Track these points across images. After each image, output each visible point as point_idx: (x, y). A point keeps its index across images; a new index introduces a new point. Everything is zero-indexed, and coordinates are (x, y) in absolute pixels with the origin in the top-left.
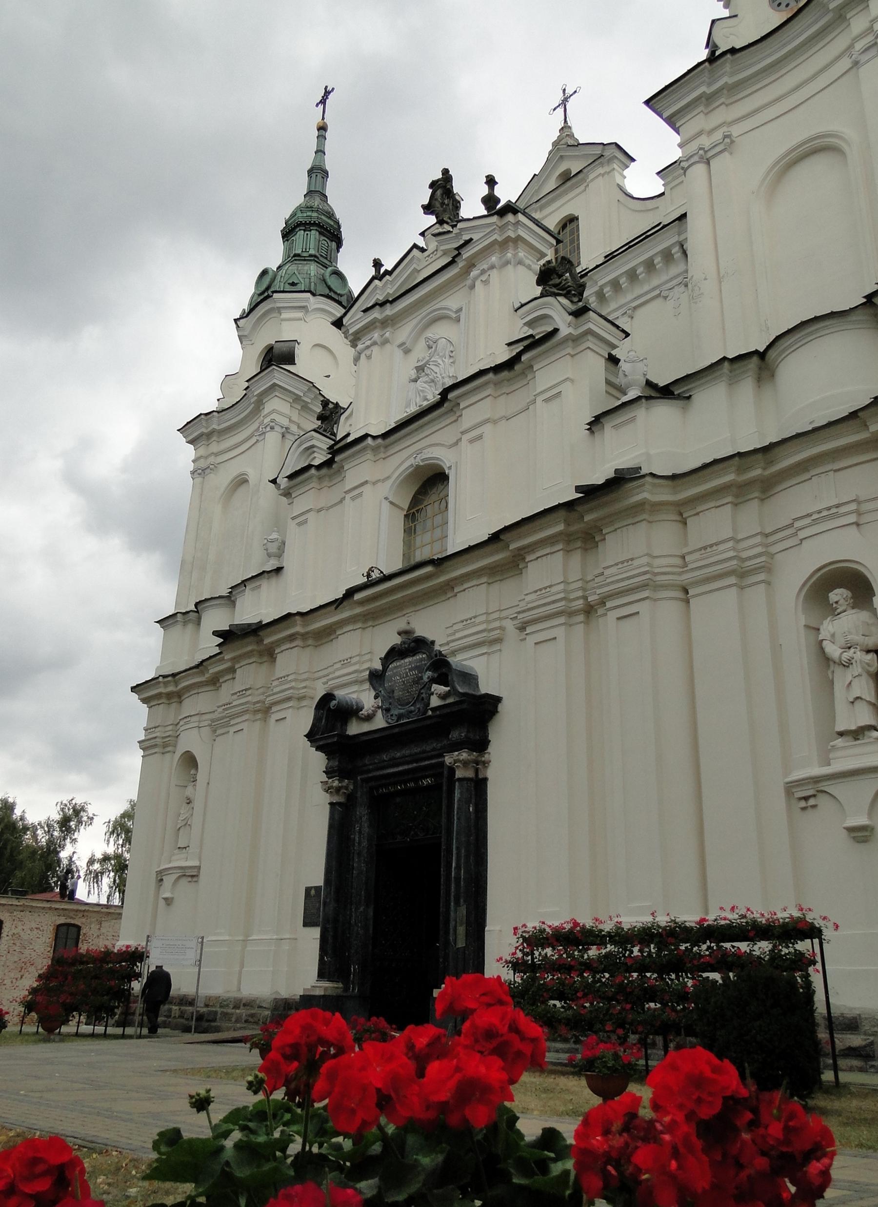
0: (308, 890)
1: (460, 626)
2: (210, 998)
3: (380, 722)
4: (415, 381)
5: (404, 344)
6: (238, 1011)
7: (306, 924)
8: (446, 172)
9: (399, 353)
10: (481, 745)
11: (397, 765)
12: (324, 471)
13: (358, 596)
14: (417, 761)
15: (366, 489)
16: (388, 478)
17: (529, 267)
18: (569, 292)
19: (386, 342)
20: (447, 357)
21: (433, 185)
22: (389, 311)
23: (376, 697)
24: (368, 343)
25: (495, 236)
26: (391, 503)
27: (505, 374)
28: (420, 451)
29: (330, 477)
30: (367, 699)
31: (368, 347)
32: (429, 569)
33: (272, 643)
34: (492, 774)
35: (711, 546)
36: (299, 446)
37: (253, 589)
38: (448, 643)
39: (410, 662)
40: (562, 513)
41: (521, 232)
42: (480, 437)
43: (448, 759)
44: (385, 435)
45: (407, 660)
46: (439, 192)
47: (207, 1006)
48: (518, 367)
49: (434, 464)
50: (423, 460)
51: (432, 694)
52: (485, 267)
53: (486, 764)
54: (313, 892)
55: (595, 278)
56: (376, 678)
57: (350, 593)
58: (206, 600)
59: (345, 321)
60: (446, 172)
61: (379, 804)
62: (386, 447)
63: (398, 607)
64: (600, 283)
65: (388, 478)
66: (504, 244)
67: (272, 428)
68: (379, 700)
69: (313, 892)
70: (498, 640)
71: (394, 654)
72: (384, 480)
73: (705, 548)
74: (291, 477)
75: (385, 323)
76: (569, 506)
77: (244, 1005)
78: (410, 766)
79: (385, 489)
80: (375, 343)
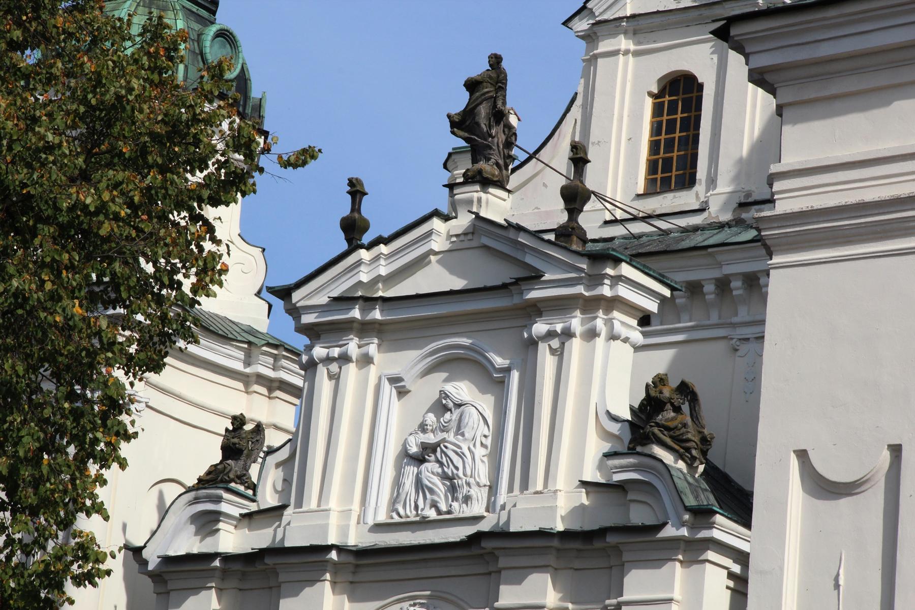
8: (496, 61)
17: (626, 340)
18: (688, 450)
20: (478, 444)
21: (472, 85)
25: (580, 289)
27: (577, 545)
41: (623, 291)
46: (483, 111)
48: (598, 544)
52: (559, 328)
55: (720, 258)
59: (296, 296)
60: (496, 61)
64: (728, 270)
66: (591, 305)
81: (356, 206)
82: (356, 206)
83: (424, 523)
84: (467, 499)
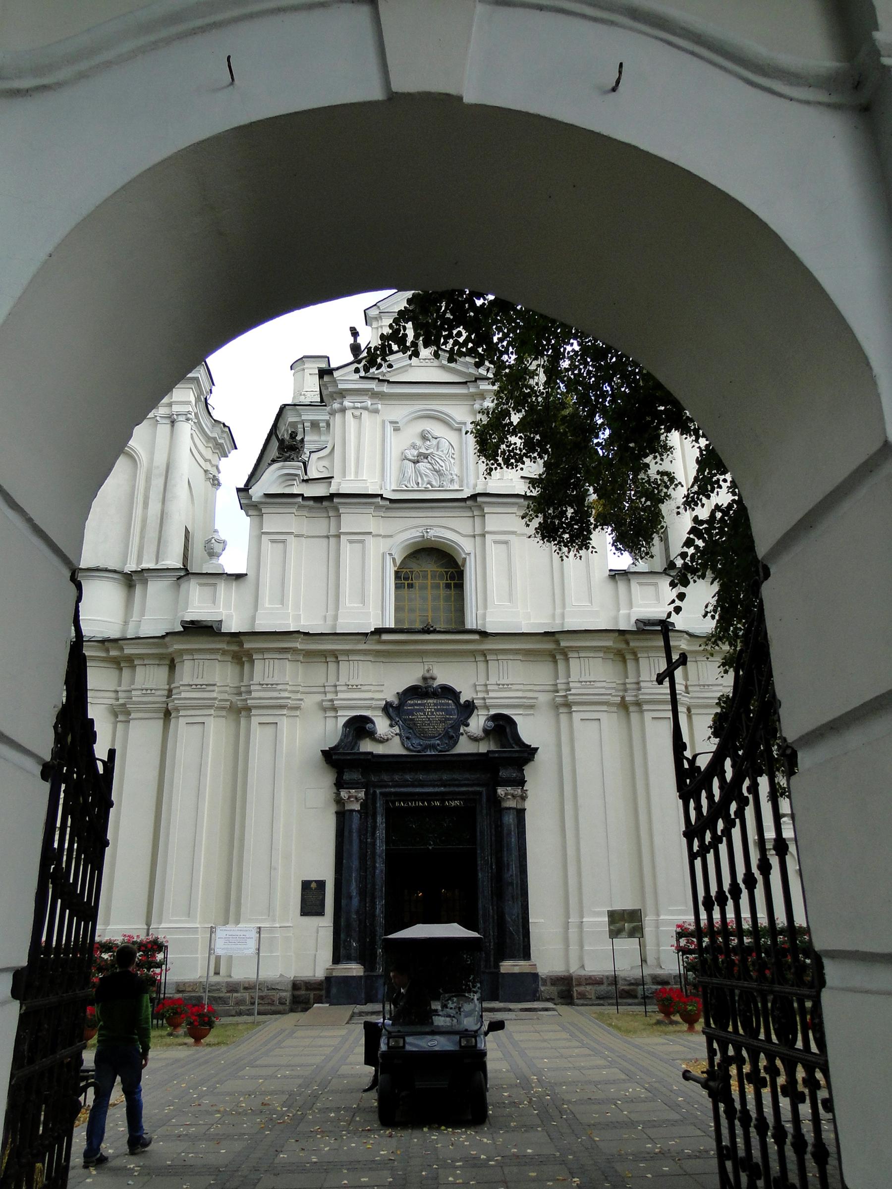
0: (306, 885)
1: (496, 687)
2: (184, 984)
3: (395, 748)
4: (415, 462)
5: (397, 423)
6: (235, 995)
7: (305, 912)
9: (389, 428)
10: (521, 782)
11: (422, 786)
12: (311, 503)
13: (385, 637)
14: (445, 786)
15: (369, 540)
16: (391, 536)
19: (376, 411)
22: (385, 388)
23: (391, 726)
24: (359, 405)
26: (394, 559)
28: (431, 527)
29: (310, 508)
30: (382, 725)
31: (357, 408)
32: (476, 637)
33: (252, 649)
34: (528, 805)
35: (708, 685)
36: (280, 469)
37: (200, 585)
38: (484, 699)
39: (435, 705)
40: (617, 634)
42: (506, 543)
43: (501, 791)
44: (391, 501)
45: (430, 701)
47: (179, 991)
49: (455, 549)
50: (434, 536)
51: (462, 734)
53: (523, 798)
54: (313, 885)
56: (387, 709)
57: (379, 632)
58: (97, 570)
61: (391, 814)
62: (388, 509)
63: (422, 654)
65: (391, 536)
67: (188, 419)
68: (396, 729)
69: (313, 885)
70: (531, 707)
71: (413, 692)
72: (385, 537)
73: (704, 686)
74: (267, 495)
75: (374, 395)
76: (622, 632)
77: (246, 988)
78: (437, 790)
79: (383, 545)
80: (366, 408)
81: (355, 340)
82: (355, 340)
83: (426, 490)
84: (452, 481)
